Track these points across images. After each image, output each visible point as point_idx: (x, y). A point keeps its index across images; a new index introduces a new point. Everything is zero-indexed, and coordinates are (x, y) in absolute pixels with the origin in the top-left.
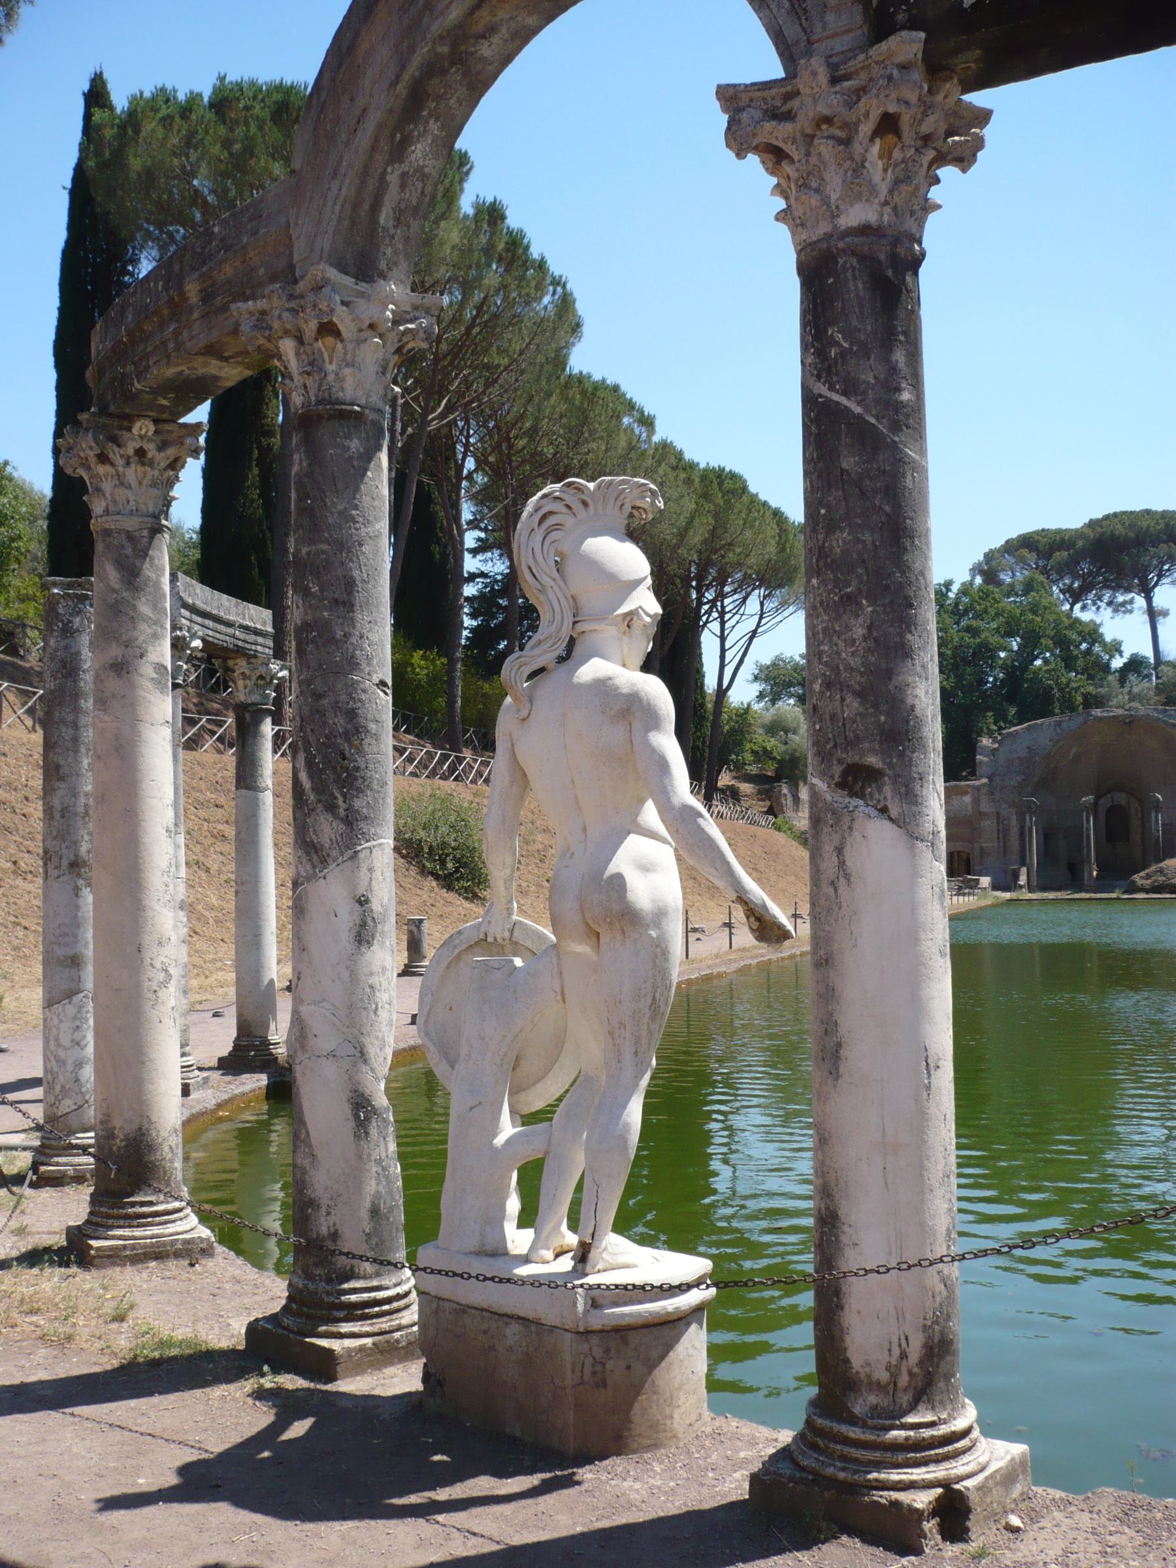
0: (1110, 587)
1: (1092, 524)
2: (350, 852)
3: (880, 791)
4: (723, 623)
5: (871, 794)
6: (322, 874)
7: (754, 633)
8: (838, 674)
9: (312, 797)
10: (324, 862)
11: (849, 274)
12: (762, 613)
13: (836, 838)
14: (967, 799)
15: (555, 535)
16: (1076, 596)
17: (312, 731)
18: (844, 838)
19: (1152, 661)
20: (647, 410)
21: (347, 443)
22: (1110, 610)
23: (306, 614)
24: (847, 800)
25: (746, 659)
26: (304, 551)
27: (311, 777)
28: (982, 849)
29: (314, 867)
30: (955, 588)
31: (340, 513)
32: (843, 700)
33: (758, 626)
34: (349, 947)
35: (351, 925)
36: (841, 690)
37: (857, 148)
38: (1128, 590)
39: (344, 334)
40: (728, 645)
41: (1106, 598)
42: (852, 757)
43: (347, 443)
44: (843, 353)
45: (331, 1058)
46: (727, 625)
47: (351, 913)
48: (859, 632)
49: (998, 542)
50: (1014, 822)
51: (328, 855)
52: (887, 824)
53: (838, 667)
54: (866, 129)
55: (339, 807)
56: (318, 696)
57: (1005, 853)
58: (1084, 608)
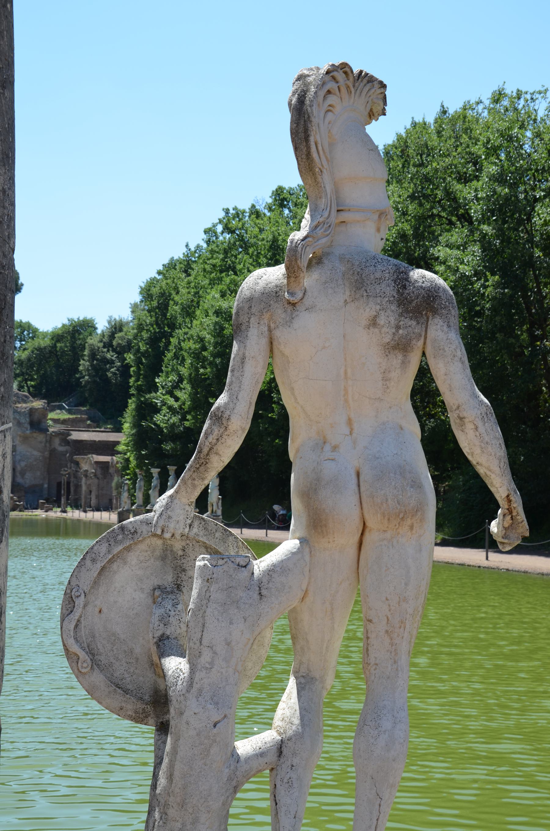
15: (330, 115)
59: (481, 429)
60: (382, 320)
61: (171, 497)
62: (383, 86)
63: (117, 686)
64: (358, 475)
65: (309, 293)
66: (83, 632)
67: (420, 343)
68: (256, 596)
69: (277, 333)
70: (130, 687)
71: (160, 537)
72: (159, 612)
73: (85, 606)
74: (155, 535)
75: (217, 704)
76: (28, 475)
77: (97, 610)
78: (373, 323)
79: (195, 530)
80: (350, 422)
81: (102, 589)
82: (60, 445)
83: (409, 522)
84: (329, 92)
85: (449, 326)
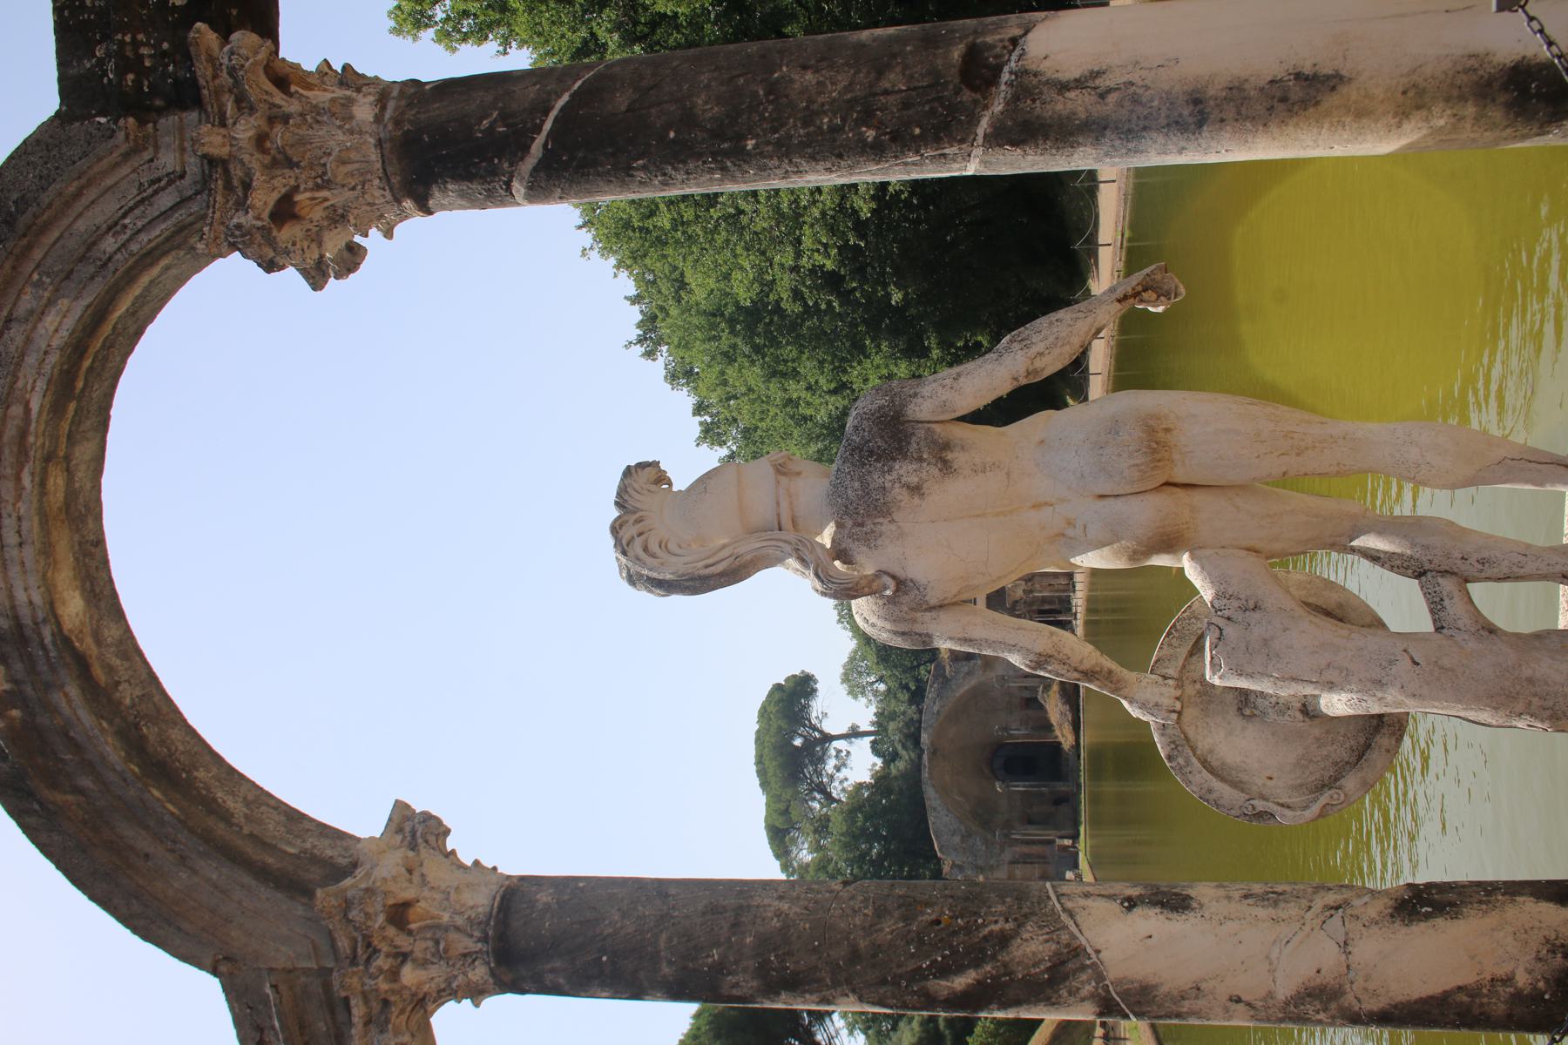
2: (1064, 917)
3: (992, 47)
5: (996, 57)
6: (1093, 955)
8: (855, 100)
9: (988, 968)
10: (1077, 952)
11: (422, 116)
13: (1049, 94)
16: (829, 797)
17: (899, 966)
18: (1047, 82)
21: (540, 906)
23: (745, 970)
24: (1003, 87)
26: (666, 970)
27: (960, 969)
29: (1083, 968)
31: (624, 915)
32: (886, 92)
34: (1192, 920)
35: (1161, 917)
36: (876, 94)
37: (293, 107)
39: (408, 894)
42: (953, 76)
43: (540, 906)
44: (504, 117)
45: (1350, 948)
47: (1146, 918)
48: (809, 76)
51: (1068, 945)
52: (1030, 36)
53: (848, 101)
54: (278, 98)
55: (1002, 931)
56: (855, 956)
59: (1040, 347)
60: (914, 480)
61: (1130, 703)
62: (628, 472)
63: (1360, 758)
64: (1102, 497)
65: (883, 568)
66: (1295, 800)
67: (937, 428)
68: (1257, 615)
69: (933, 602)
70: (1362, 740)
71: (1180, 713)
72: (1272, 716)
73: (1263, 798)
74: (1178, 721)
75: (1391, 662)
77: (1269, 783)
78: (916, 490)
79: (1171, 672)
80: (1037, 506)
81: (1245, 778)
83: (1161, 435)
84: (646, 549)
85: (916, 395)
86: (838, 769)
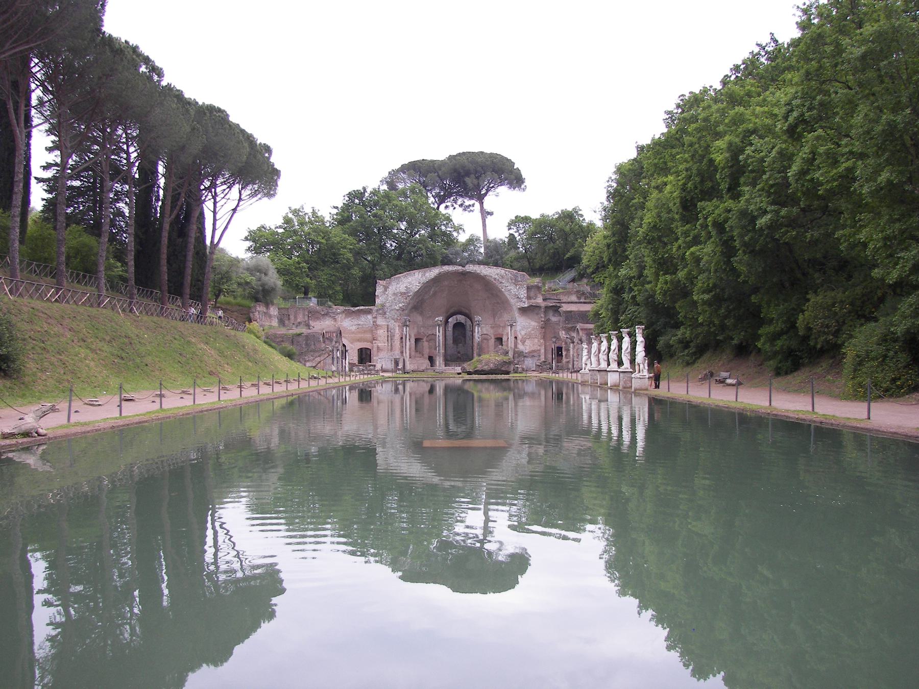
0: (461, 196)
1: (451, 158)
4: (215, 203)
7: (234, 210)
12: (240, 199)
14: (369, 317)
19: (482, 239)
20: (158, 64)
22: (461, 209)
25: (229, 226)
28: (378, 347)
30: (369, 190)
33: (238, 206)
38: (471, 198)
40: (218, 217)
41: (459, 202)
46: (218, 205)
49: (397, 166)
50: (397, 331)
57: (391, 349)
58: (447, 207)
76: (528, 342)
82: (554, 315)
86: (461, 205)
